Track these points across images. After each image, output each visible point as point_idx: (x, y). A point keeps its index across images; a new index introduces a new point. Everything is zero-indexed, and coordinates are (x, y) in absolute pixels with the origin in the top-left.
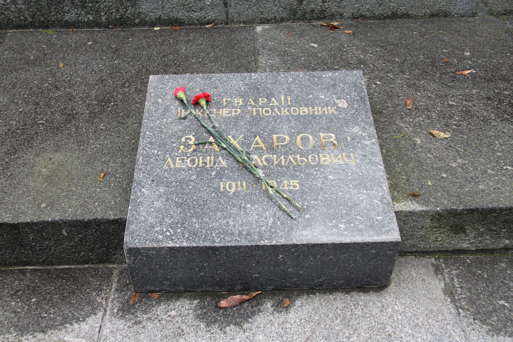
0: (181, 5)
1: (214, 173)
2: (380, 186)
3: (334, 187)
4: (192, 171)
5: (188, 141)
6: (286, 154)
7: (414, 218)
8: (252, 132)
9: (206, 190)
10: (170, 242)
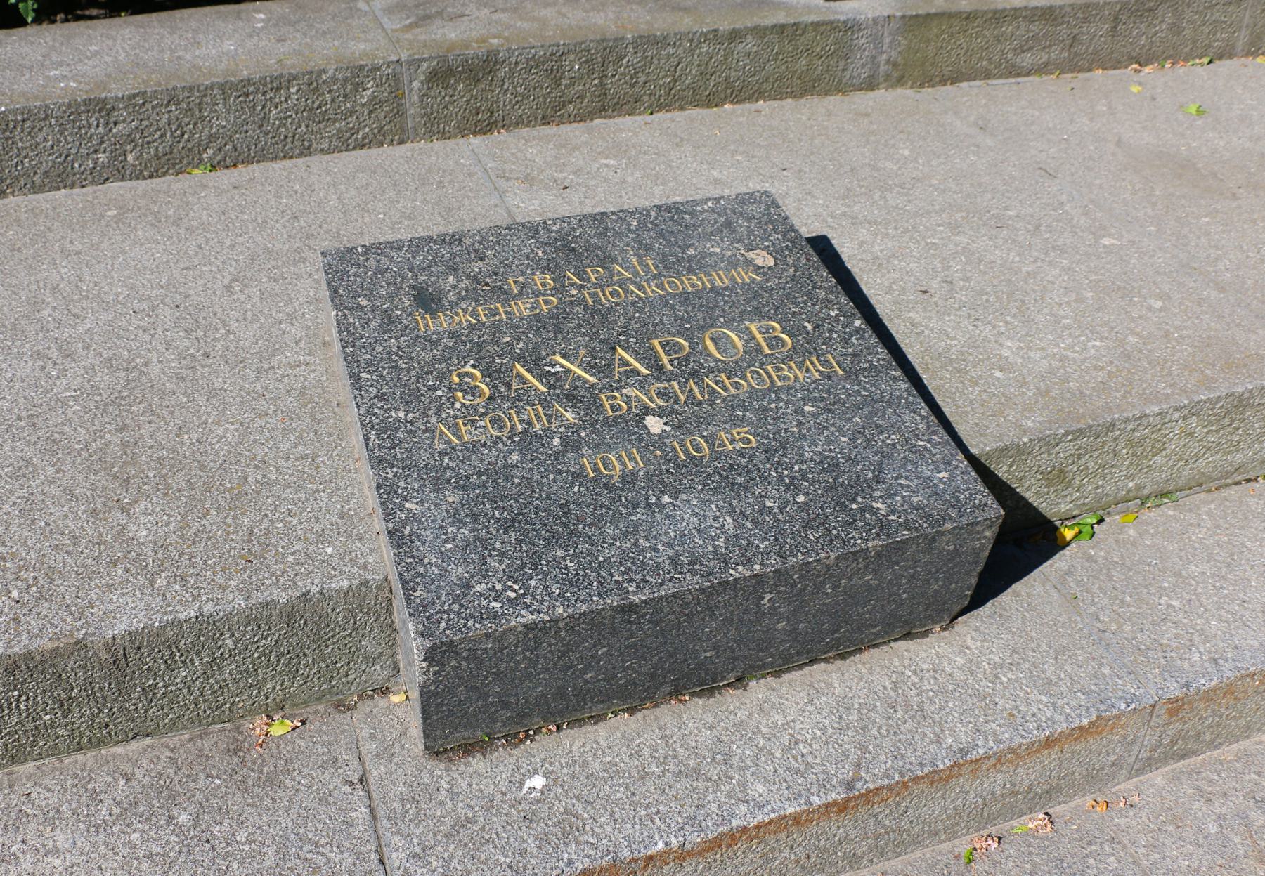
1: (556, 441)
2: (914, 411)
3: (826, 428)
8: (603, 341)
9: (554, 481)
10: (523, 612)
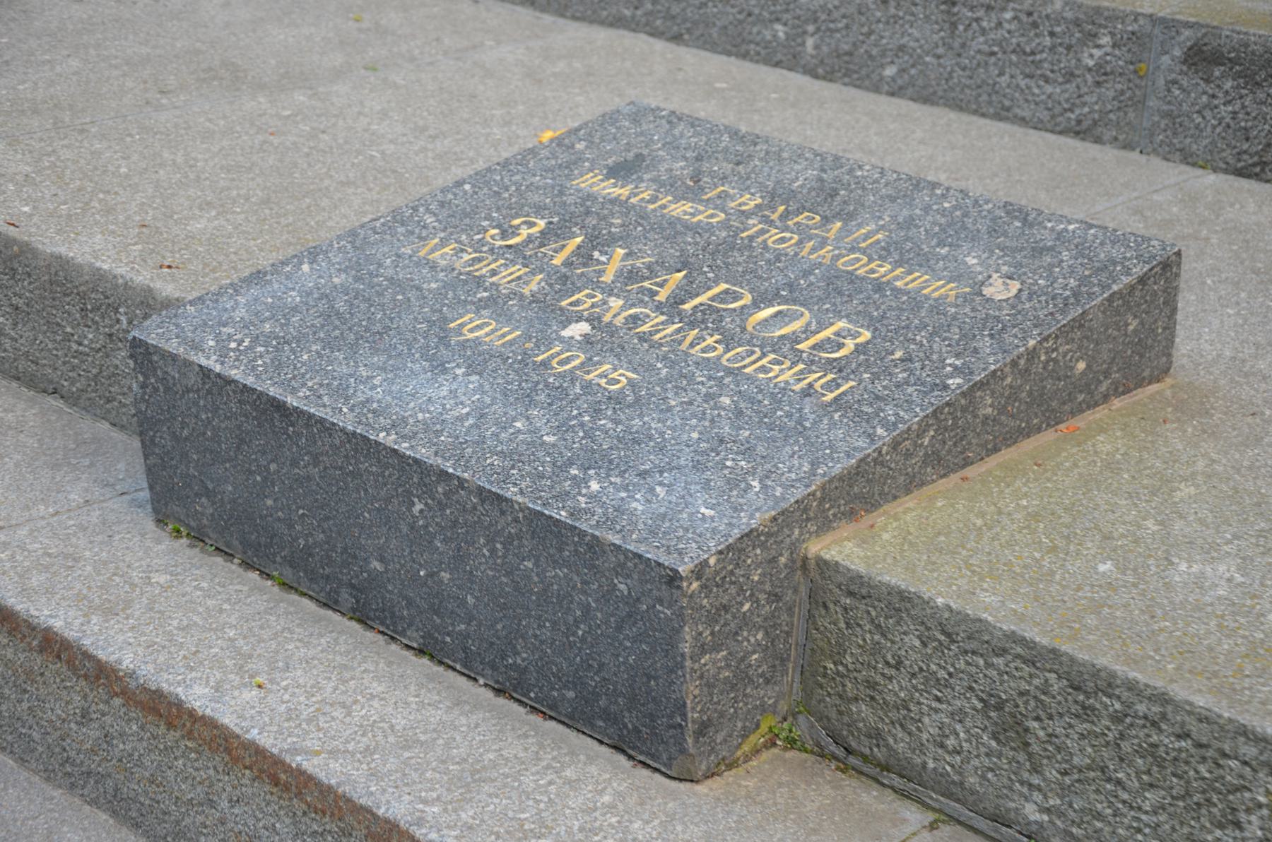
0: (1014, 51)
7: (874, 613)
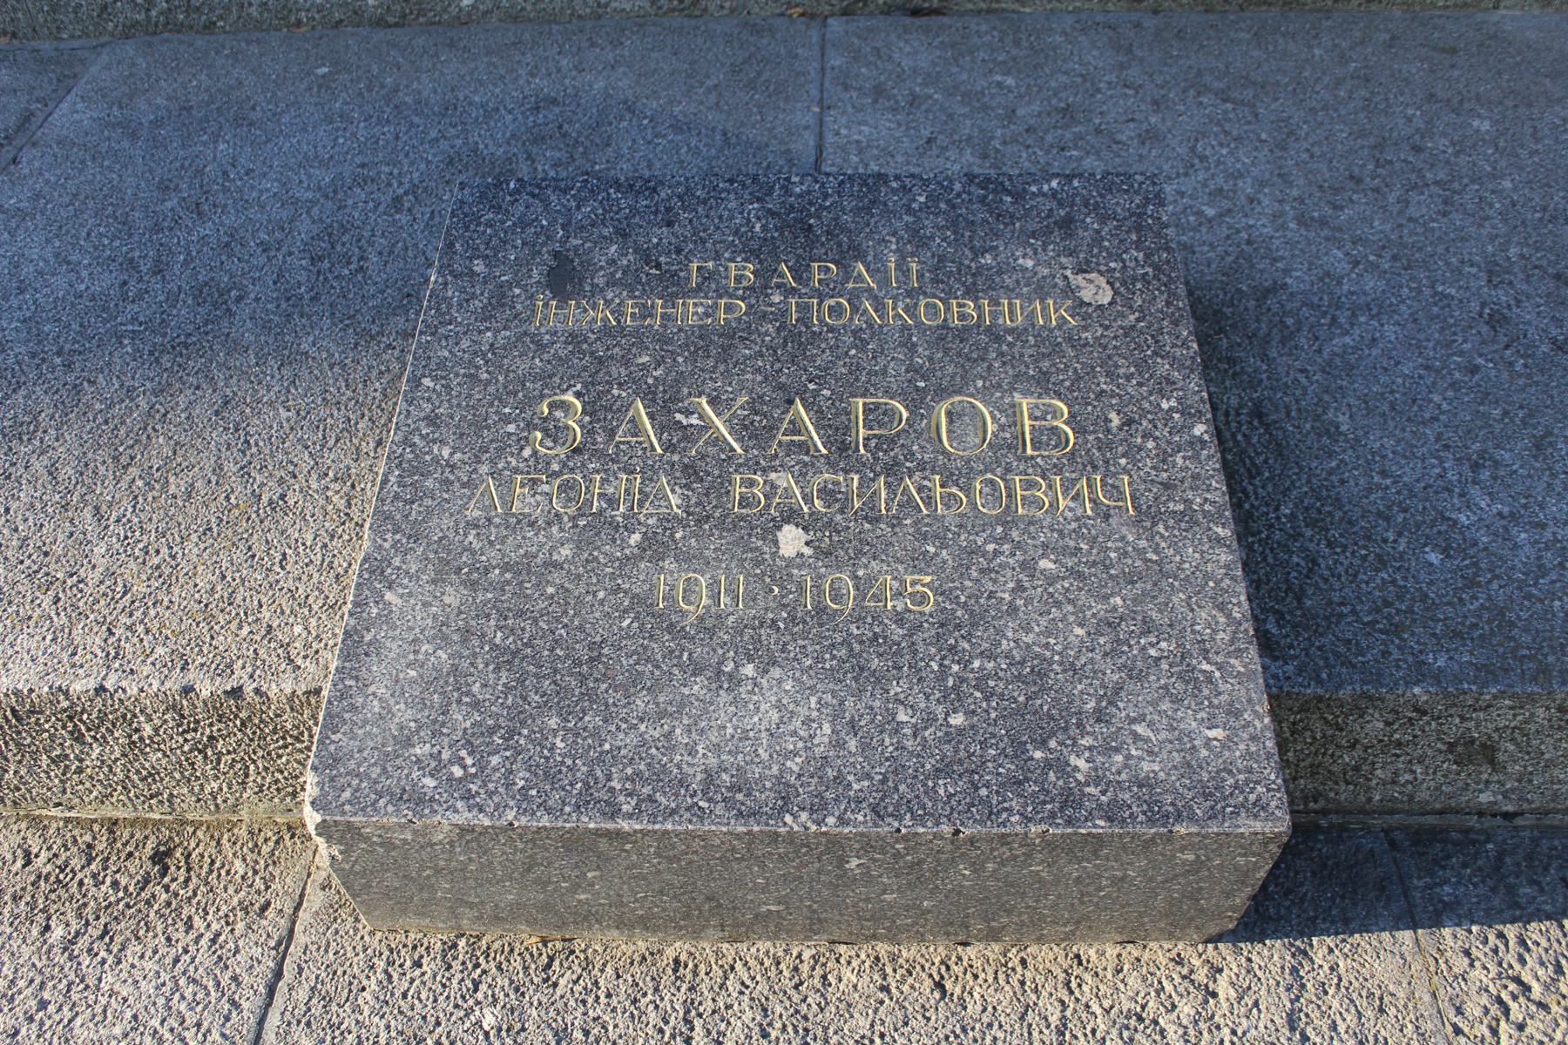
2: (1221, 607)
3: (1058, 604)
4: (561, 530)
5: (559, 414)
6: (892, 470)
8: (781, 387)
9: (602, 602)
10: (459, 804)
